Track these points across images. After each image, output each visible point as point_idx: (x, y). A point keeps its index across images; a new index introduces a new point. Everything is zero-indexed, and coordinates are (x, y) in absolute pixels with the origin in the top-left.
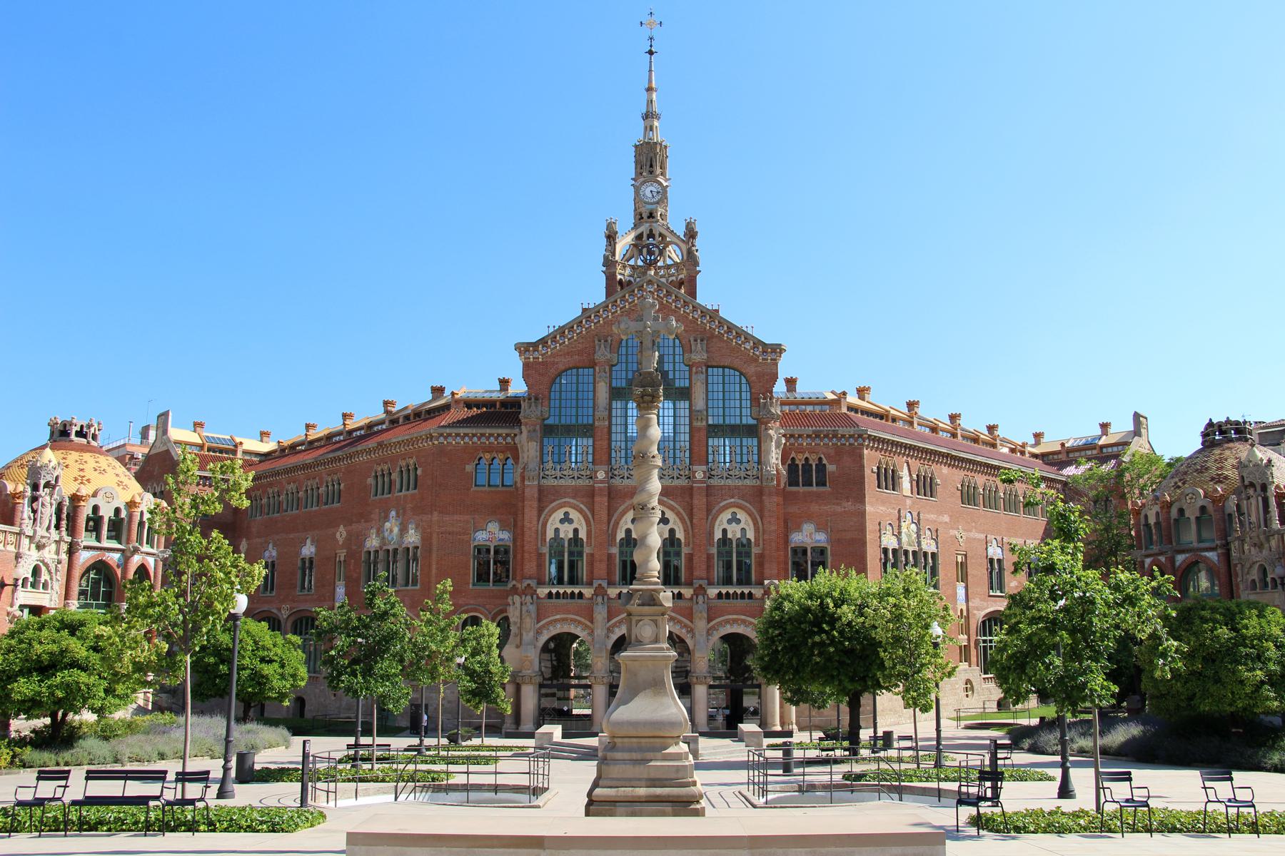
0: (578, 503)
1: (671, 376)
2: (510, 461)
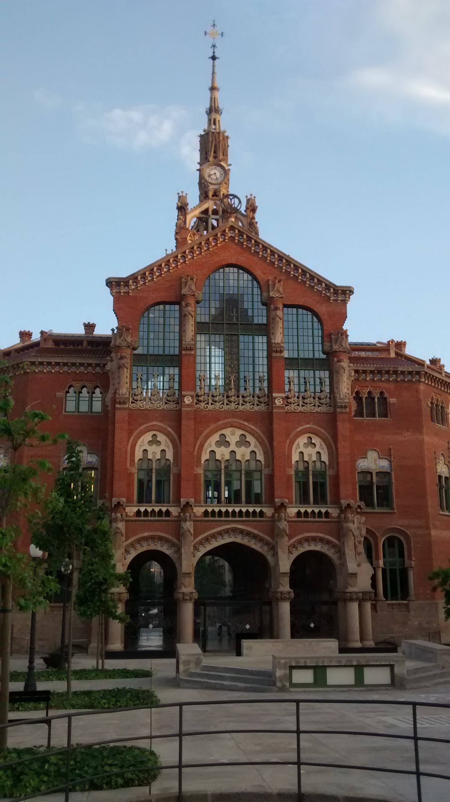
0: (165, 427)
1: (250, 314)
2: (98, 391)
